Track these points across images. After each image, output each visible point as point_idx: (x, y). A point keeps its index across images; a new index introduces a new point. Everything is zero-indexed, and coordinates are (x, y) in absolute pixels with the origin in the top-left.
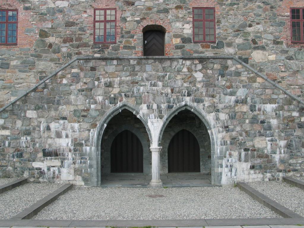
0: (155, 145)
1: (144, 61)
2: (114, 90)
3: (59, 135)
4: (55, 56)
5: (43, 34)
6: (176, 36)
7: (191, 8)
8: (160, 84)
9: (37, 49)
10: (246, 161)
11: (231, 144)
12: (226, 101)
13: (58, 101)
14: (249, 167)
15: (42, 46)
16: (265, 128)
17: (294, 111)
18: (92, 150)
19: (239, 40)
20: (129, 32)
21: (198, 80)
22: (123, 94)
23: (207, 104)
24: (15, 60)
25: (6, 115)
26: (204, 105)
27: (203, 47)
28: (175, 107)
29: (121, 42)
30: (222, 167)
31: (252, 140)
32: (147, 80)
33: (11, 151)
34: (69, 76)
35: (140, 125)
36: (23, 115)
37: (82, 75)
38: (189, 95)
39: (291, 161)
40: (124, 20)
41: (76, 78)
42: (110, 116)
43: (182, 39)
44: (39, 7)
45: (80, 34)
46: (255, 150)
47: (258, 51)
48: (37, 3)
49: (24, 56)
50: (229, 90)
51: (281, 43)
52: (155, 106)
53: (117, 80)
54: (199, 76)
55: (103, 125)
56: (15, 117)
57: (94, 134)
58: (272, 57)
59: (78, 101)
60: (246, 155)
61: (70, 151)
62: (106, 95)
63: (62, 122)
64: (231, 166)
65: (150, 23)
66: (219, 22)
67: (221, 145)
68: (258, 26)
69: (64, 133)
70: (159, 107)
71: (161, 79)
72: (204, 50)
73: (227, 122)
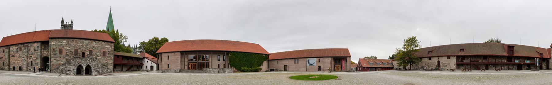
16: (99, 68)
18: (75, 70)
35: (82, 67)
59: (74, 63)
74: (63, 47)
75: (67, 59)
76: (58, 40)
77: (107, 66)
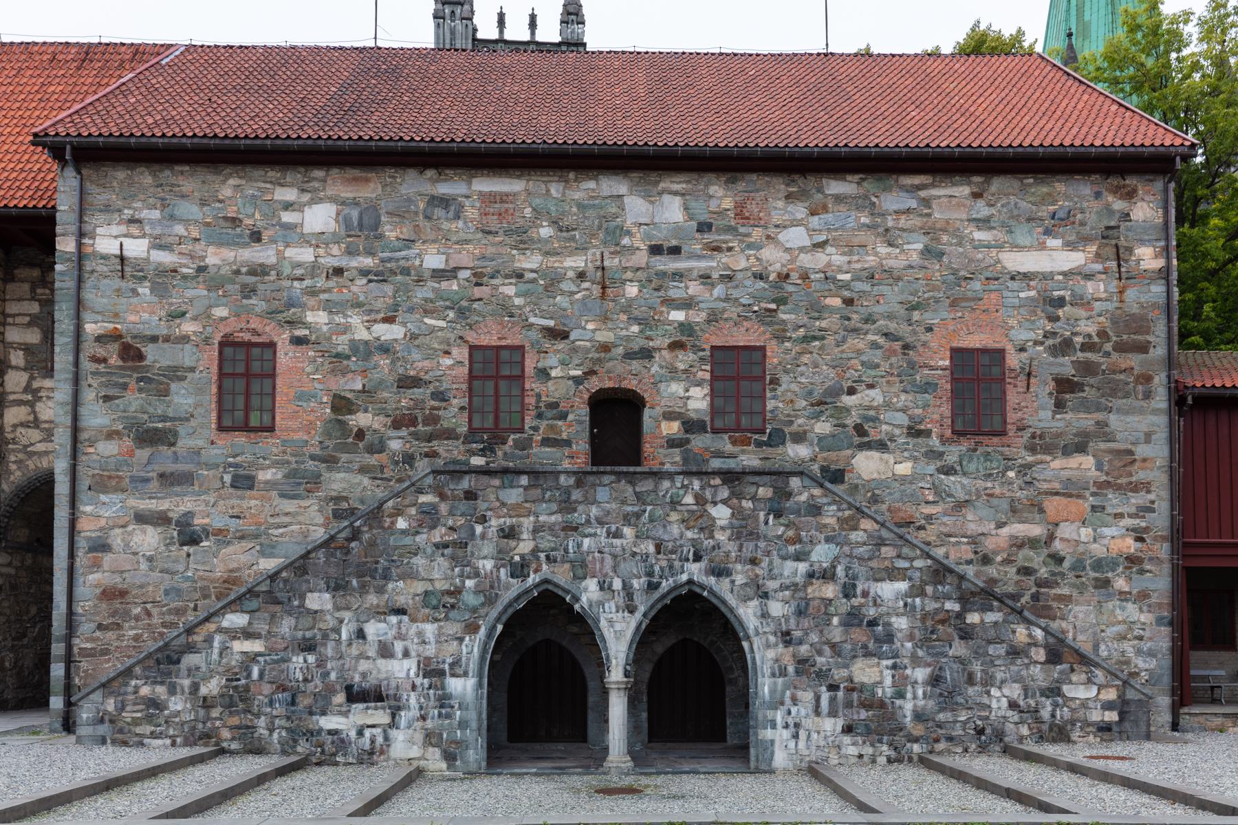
0: (616, 675)
1: (591, 478)
2: (522, 544)
3: (385, 651)
4: (373, 460)
5: (342, 405)
6: (669, 416)
7: (707, 347)
8: (628, 531)
9: (327, 443)
10: (833, 713)
11: (797, 672)
12: (786, 574)
13: (386, 569)
14: (839, 729)
15: (339, 434)
16: (878, 638)
17: (948, 597)
19: (823, 427)
20: (555, 405)
21: (719, 523)
22: (542, 555)
23: (740, 579)
24: (269, 467)
25: (254, 604)
26: (733, 582)
27: (734, 443)
28: (665, 585)
29: (536, 429)
30: (774, 726)
31: (846, 666)
32: (601, 522)
33: (267, 689)
34: (413, 511)
35: (582, 628)
36: (296, 603)
37: (444, 508)
38: (697, 558)
39: (941, 717)
40: (544, 374)
41: (429, 518)
42: (510, 605)
43: (683, 423)
44: (330, 338)
45: (433, 408)
46: (853, 690)
47: (869, 453)
48: (325, 328)
49: (293, 459)
50: (791, 549)
51: (927, 433)
52: (617, 584)
53: (528, 523)
54: (721, 513)
55: (494, 627)
56: (278, 608)
57: (473, 648)
58: (904, 468)
59: (438, 572)
60: (833, 700)
61: (414, 687)
62: (501, 556)
63: (394, 619)
64: (797, 725)
65: (608, 384)
66: (775, 382)
67: (773, 675)
68: (872, 393)
69: (399, 647)
70: (626, 586)
71: (633, 520)
72: (737, 449)
73: (787, 621)
74: (285, 312)
75: (341, 510)
76: (199, 198)
77: (1041, 609)
